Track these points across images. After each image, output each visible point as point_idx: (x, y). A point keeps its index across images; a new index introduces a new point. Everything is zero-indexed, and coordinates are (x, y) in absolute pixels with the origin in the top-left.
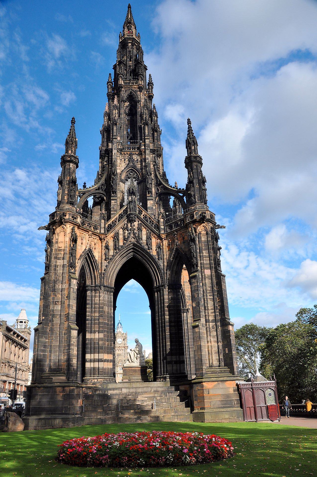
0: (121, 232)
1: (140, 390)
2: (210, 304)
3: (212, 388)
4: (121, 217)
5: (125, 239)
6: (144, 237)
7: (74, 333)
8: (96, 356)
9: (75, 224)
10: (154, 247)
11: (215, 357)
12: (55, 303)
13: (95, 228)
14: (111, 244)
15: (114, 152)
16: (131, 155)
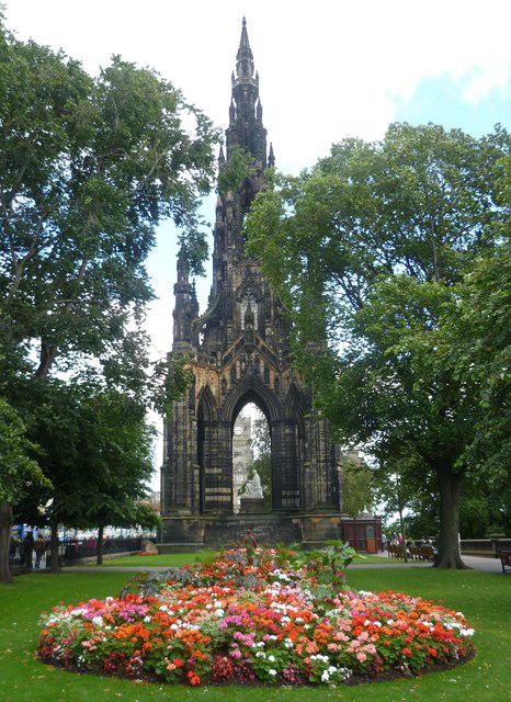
0: (238, 364)
1: (256, 522)
2: (322, 444)
3: (319, 523)
4: (237, 347)
5: (242, 372)
6: (262, 370)
7: (197, 472)
8: (216, 490)
9: (193, 363)
10: (272, 381)
11: (324, 495)
12: (177, 444)
13: (212, 362)
14: (228, 377)
15: (230, 266)
16: (248, 267)
